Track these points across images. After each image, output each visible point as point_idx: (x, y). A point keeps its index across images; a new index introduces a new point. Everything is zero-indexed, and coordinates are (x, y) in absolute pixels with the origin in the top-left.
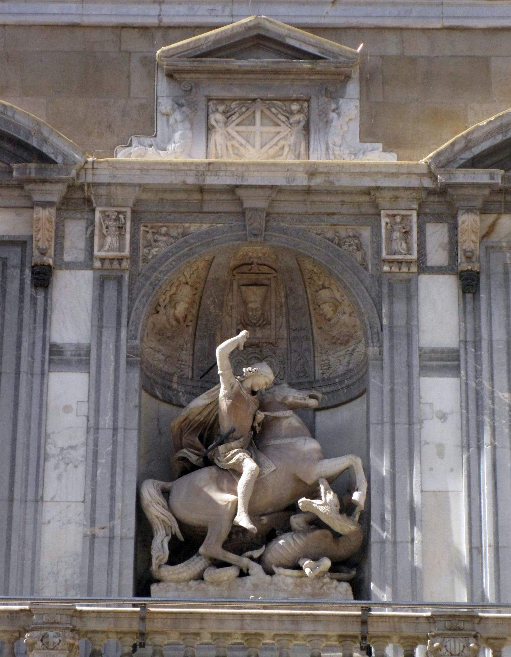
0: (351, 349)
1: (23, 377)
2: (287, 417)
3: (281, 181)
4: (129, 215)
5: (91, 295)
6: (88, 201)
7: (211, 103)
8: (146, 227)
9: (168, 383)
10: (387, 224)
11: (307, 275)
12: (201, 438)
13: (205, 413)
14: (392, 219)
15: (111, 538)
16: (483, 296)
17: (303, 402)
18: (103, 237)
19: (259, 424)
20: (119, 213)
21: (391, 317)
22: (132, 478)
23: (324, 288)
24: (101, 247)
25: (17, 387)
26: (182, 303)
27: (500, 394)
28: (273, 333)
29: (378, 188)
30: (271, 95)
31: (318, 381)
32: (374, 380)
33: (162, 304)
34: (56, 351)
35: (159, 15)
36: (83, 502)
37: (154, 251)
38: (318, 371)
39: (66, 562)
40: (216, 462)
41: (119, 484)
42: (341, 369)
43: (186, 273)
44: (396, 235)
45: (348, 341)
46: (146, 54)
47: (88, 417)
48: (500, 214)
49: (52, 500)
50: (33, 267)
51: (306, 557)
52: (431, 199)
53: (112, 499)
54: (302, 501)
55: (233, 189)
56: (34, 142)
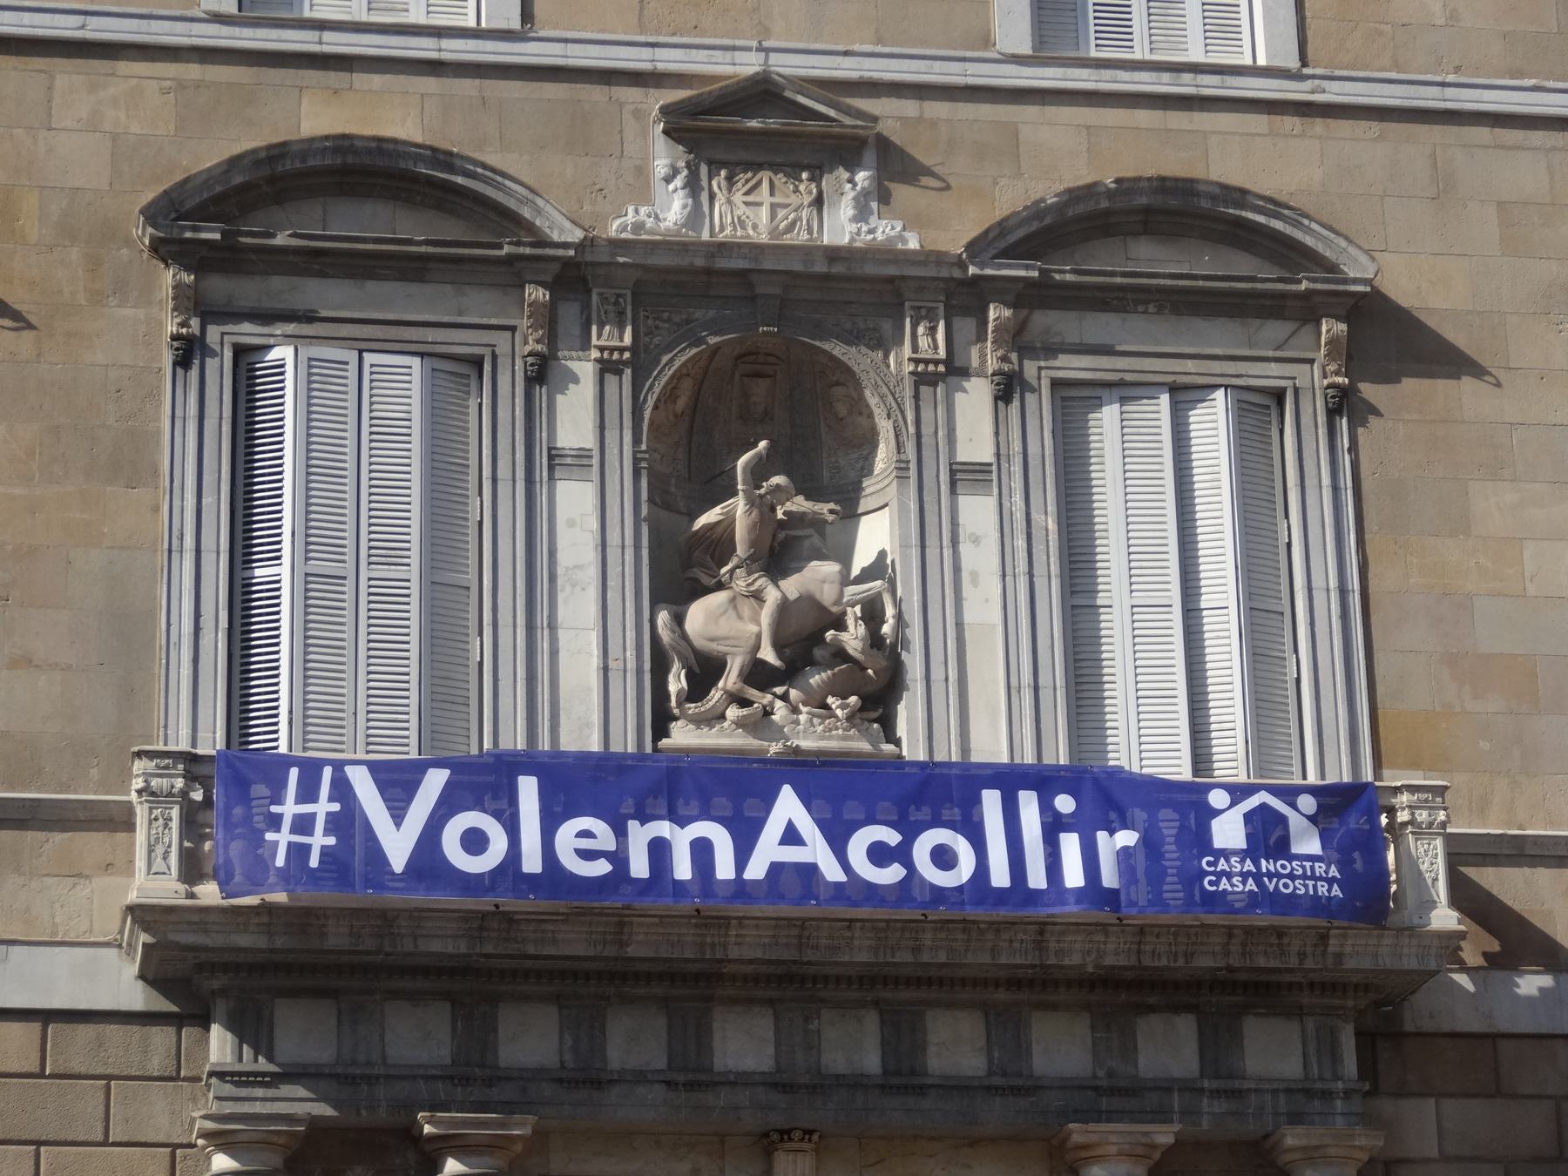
2: (807, 537)
3: (798, 267)
4: (629, 299)
6: (584, 280)
20: (618, 296)
23: (838, 384)
24: (599, 336)
29: (903, 278)
37: (656, 340)
38: (826, 474)
55: (743, 274)
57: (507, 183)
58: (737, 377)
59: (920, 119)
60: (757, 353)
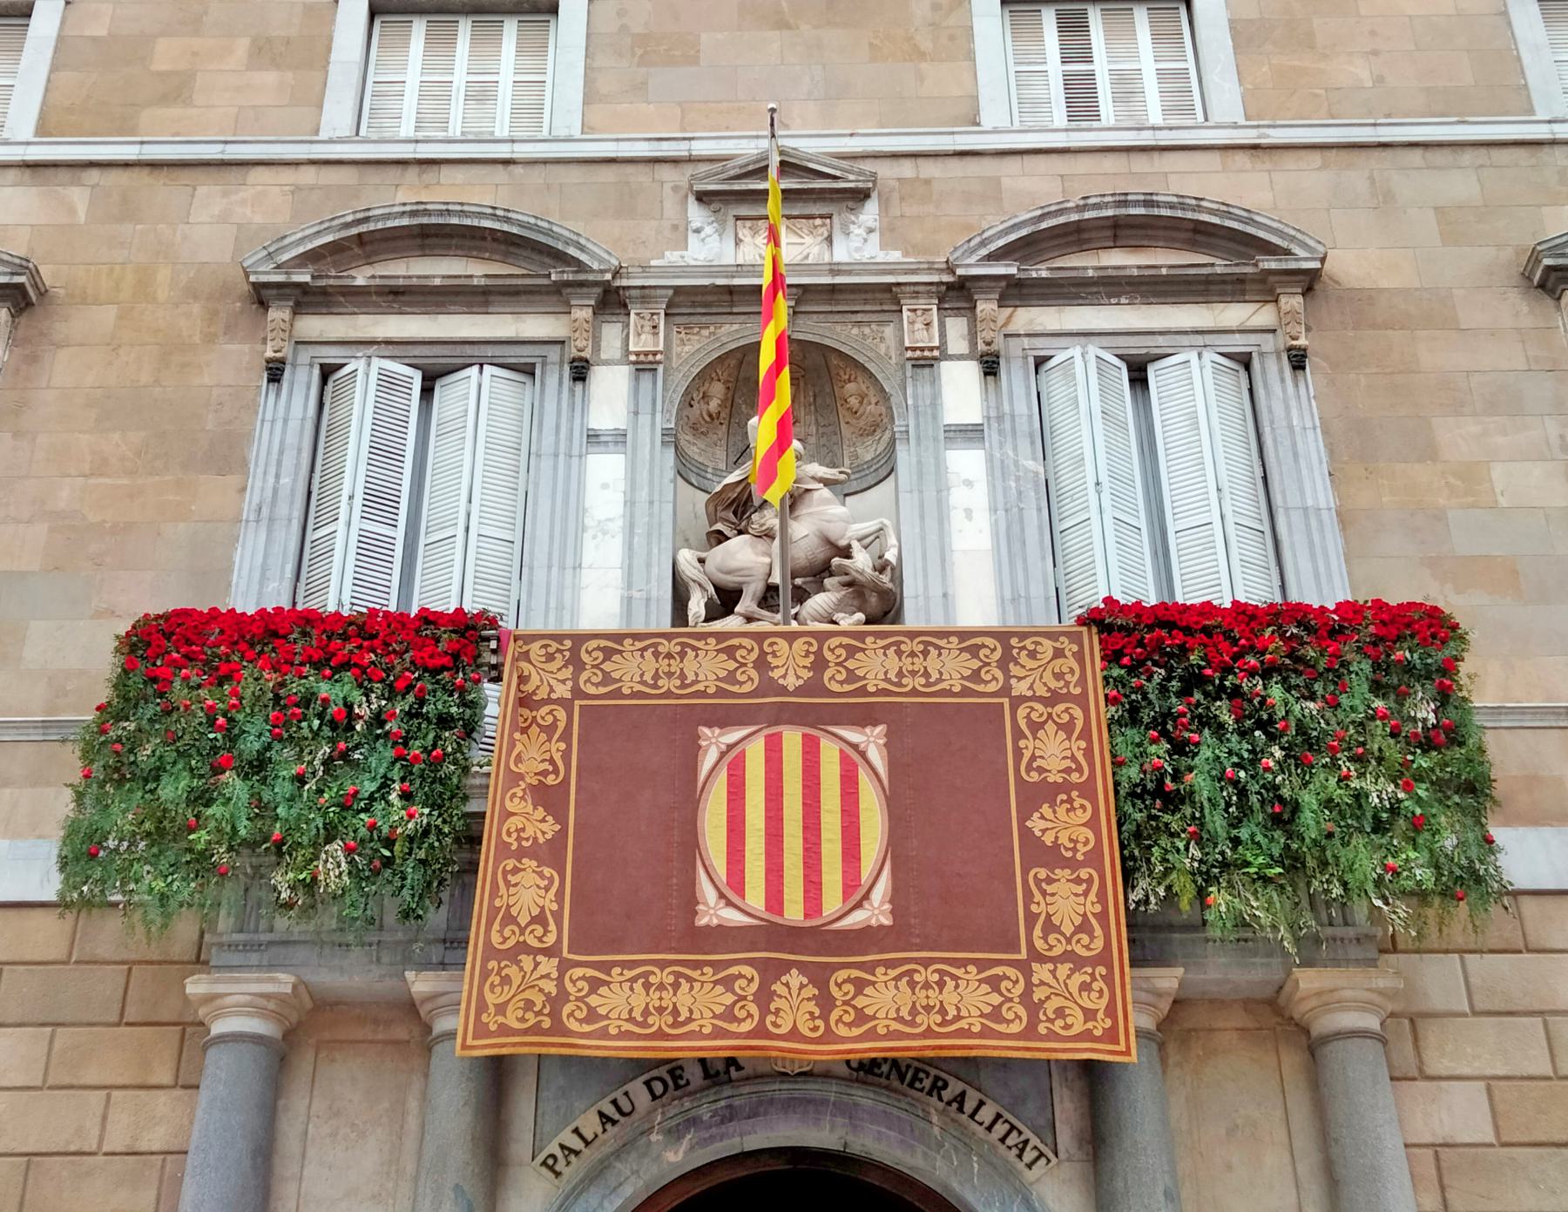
1: (561, 457)
6: (625, 306)
11: (833, 372)
12: (735, 513)
15: (648, 600)
21: (915, 397)
22: (667, 545)
24: (636, 344)
25: (555, 468)
29: (899, 284)
32: (904, 456)
37: (687, 348)
41: (655, 551)
42: (868, 457)
52: (951, 294)
53: (649, 565)
56: (572, 251)
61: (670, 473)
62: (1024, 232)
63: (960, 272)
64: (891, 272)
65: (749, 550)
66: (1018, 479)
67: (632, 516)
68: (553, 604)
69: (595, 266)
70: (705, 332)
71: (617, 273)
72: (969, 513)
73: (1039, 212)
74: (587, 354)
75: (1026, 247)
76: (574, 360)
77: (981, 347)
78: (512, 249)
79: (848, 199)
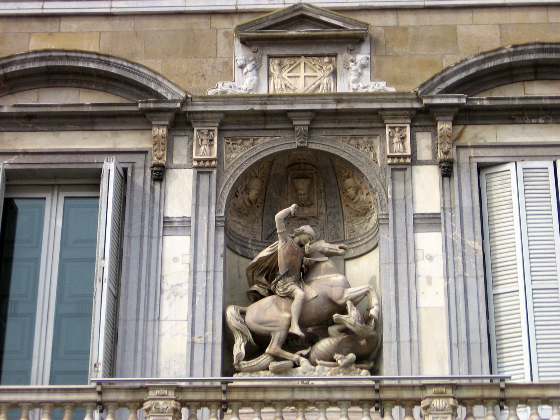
0: (368, 218)
1: (146, 239)
5: (192, 185)
7: (271, 60)
8: (228, 140)
9: (245, 244)
10: (390, 133)
12: (266, 278)
13: (269, 261)
14: (393, 130)
16: (456, 178)
17: (335, 251)
18: (199, 146)
19: (306, 267)
20: (209, 131)
23: (348, 177)
24: (197, 154)
26: (253, 190)
27: (469, 242)
28: (316, 210)
29: (383, 109)
30: (311, 53)
31: (346, 240)
33: (240, 191)
34: (167, 222)
35: (236, 5)
36: (187, 320)
37: (233, 156)
39: (175, 360)
40: (277, 292)
43: (255, 171)
44: (395, 140)
45: (366, 213)
46: (227, 30)
47: (189, 265)
48: (465, 125)
49: (165, 320)
50: (152, 167)
51: (339, 352)
54: (335, 316)
56: (153, 86)
57: (141, 70)
58: (289, 179)
59: (397, 27)
60: (300, 163)
61: (221, 250)
62: (472, 71)
63: (425, 101)
64: (378, 101)
65: (275, 308)
66: (463, 255)
67: (195, 282)
68: (140, 347)
69: (169, 97)
70: (247, 143)
71: (185, 102)
72: (429, 280)
73: (482, 57)
74: (163, 162)
75: (475, 82)
76: (154, 166)
77: (441, 156)
78: (110, 83)
79: (348, 43)
